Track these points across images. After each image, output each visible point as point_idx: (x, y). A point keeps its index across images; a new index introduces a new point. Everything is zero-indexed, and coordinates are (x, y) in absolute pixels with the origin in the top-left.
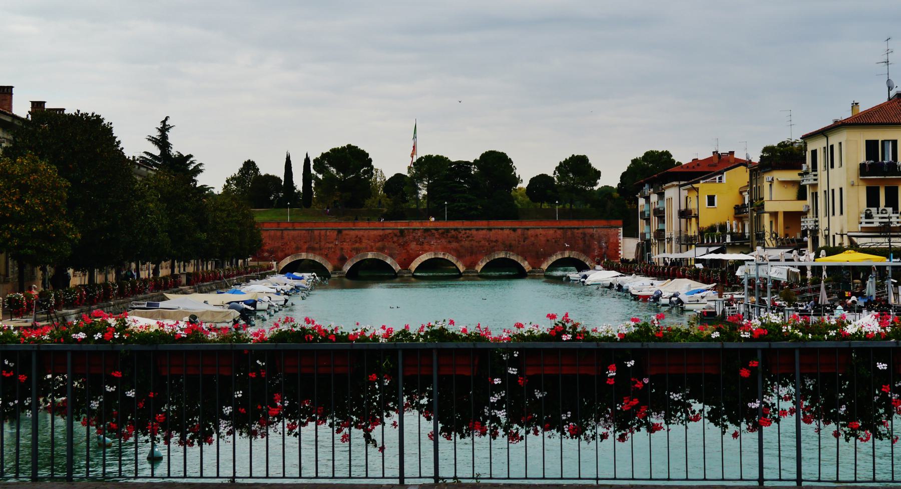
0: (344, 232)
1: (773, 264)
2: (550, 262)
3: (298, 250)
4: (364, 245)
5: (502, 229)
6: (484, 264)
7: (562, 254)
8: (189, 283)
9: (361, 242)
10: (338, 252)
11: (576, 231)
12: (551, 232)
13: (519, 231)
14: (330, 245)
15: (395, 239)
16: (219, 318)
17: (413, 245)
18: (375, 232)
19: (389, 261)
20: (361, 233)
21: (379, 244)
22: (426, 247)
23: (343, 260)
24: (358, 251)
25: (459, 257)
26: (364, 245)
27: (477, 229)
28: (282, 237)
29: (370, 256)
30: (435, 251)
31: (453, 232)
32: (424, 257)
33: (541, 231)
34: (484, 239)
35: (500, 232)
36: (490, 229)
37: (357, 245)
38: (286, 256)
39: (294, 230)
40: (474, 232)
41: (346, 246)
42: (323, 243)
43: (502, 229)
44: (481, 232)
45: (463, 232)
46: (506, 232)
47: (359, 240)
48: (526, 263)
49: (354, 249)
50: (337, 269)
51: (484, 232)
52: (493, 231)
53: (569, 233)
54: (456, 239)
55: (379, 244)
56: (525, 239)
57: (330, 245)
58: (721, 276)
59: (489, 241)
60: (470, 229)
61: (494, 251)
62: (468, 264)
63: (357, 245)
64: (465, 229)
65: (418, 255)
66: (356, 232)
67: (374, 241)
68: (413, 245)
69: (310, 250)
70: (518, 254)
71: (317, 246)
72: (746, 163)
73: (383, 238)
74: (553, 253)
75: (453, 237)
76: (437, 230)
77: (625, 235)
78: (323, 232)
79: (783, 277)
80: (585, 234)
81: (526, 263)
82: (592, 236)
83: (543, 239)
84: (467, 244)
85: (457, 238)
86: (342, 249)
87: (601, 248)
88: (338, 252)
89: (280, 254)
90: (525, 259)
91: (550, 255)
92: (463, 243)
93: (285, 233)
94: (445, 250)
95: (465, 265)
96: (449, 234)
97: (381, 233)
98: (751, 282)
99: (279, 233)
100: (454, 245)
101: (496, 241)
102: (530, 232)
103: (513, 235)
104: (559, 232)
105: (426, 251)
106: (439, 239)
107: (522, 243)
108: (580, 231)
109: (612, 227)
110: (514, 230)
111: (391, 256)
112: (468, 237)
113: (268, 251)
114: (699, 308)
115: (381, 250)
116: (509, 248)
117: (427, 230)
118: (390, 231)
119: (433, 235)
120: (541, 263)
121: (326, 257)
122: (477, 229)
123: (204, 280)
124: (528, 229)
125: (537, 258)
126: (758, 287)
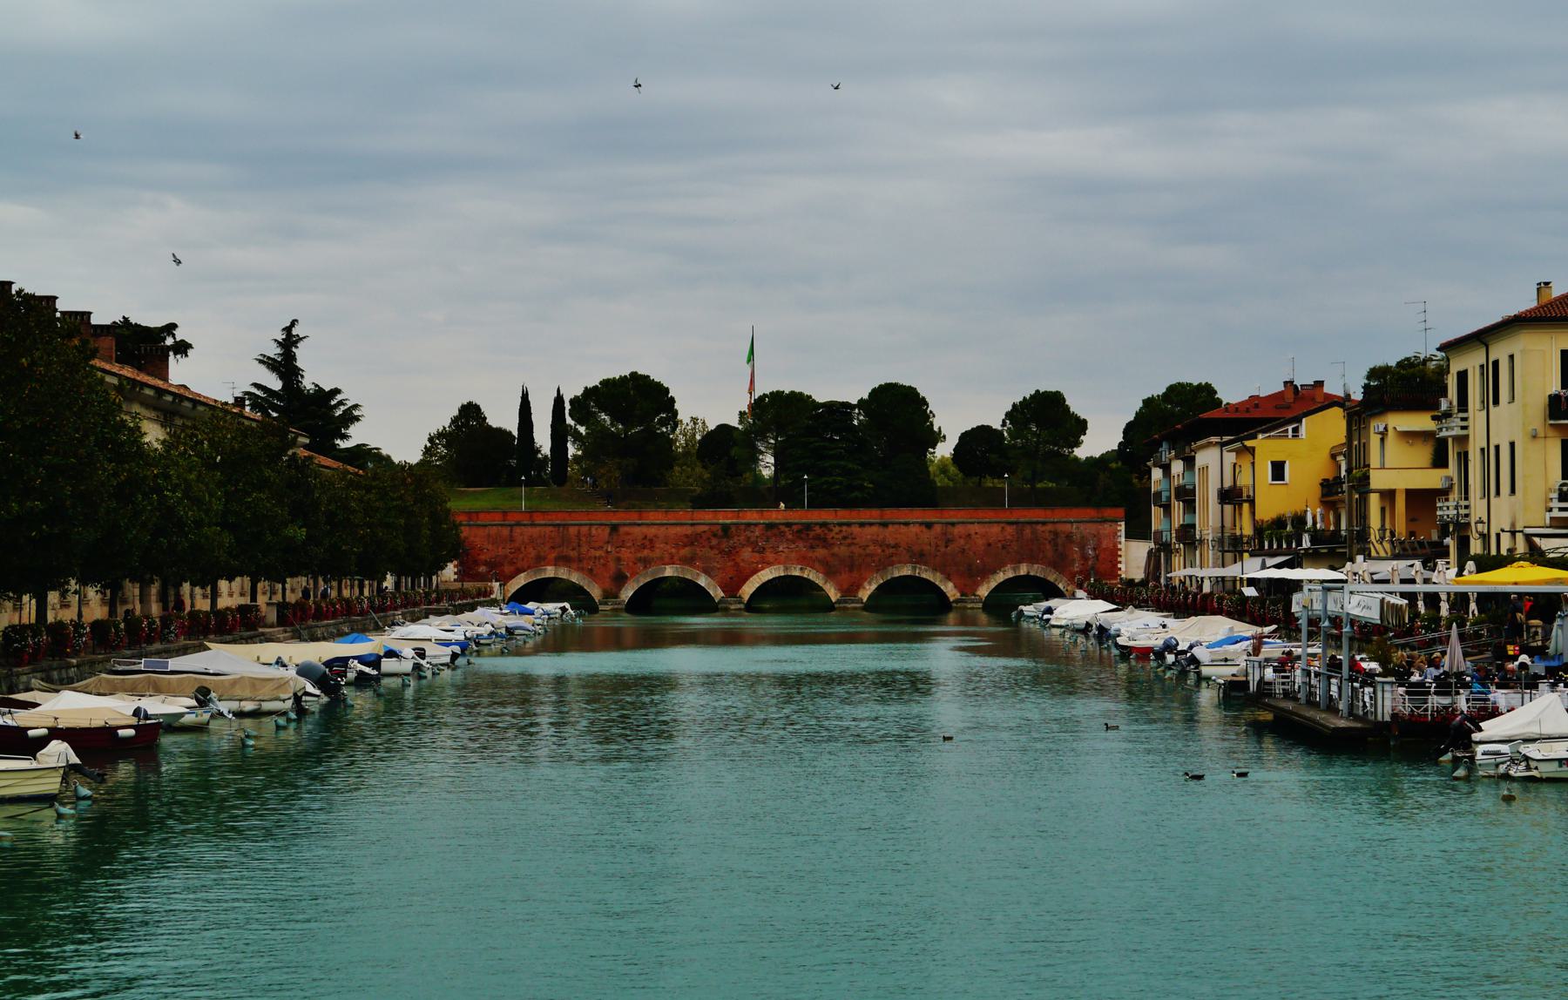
0: (623, 530)
1: (1364, 591)
2: (993, 584)
3: (540, 561)
4: (657, 553)
5: (907, 524)
6: (874, 587)
7: (1014, 569)
8: (282, 621)
9: (652, 548)
10: (612, 565)
11: (1039, 527)
12: (996, 529)
13: (938, 528)
14: (598, 553)
15: (714, 542)
16: (265, 692)
17: (747, 553)
18: (679, 529)
19: (703, 581)
20: (653, 531)
21: (686, 551)
22: (770, 556)
23: (620, 580)
24: (646, 562)
25: (829, 573)
26: (657, 553)
27: (862, 525)
28: (512, 539)
29: (669, 571)
30: (786, 563)
31: (818, 530)
32: (766, 575)
33: (976, 528)
34: (875, 542)
35: (903, 529)
36: (885, 525)
37: (646, 553)
39: (533, 525)
40: (856, 530)
41: (626, 554)
42: (584, 549)
43: (907, 524)
44: (868, 530)
45: (837, 529)
46: (914, 529)
47: (650, 543)
48: (950, 585)
49: (640, 560)
50: (610, 595)
51: (875, 529)
53: (1028, 531)
54: (824, 542)
55: (686, 551)
56: (948, 542)
57: (598, 553)
58: (1270, 607)
59: (883, 544)
60: (849, 525)
61: (892, 564)
63: (646, 553)
64: (840, 525)
65: (755, 571)
66: (644, 529)
67: (677, 546)
68: (747, 553)
69: (562, 560)
70: (935, 569)
71: (573, 554)
72: (1341, 402)
73: (692, 540)
75: (817, 537)
76: (789, 525)
77: (1129, 536)
78: (584, 529)
79: (1374, 615)
80: (1056, 534)
81: (950, 585)
82: (1069, 536)
83: (980, 542)
84: (843, 551)
85: (825, 540)
86: (619, 559)
87: (1085, 558)
88: (612, 565)
89: (507, 569)
90: (949, 578)
91: (994, 572)
92: (836, 549)
93: (518, 530)
94: (804, 561)
95: (840, 589)
96: (812, 534)
97: (689, 530)
98: (1314, 622)
99: (506, 531)
100: (821, 552)
101: (896, 546)
102: (957, 530)
103: (927, 536)
104: (1010, 529)
105: (769, 564)
108: (1049, 527)
109: (1105, 521)
110: (929, 526)
111: (707, 572)
112: (845, 538)
113: (486, 563)
114: (1223, 673)
115: (689, 561)
116: (919, 558)
117: (770, 526)
118: (706, 528)
119: (782, 534)
120: (977, 585)
121: (590, 573)
122: (862, 525)
123: (319, 615)
124: (953, 524)
125: (970, 576)
126: (1330, 629)
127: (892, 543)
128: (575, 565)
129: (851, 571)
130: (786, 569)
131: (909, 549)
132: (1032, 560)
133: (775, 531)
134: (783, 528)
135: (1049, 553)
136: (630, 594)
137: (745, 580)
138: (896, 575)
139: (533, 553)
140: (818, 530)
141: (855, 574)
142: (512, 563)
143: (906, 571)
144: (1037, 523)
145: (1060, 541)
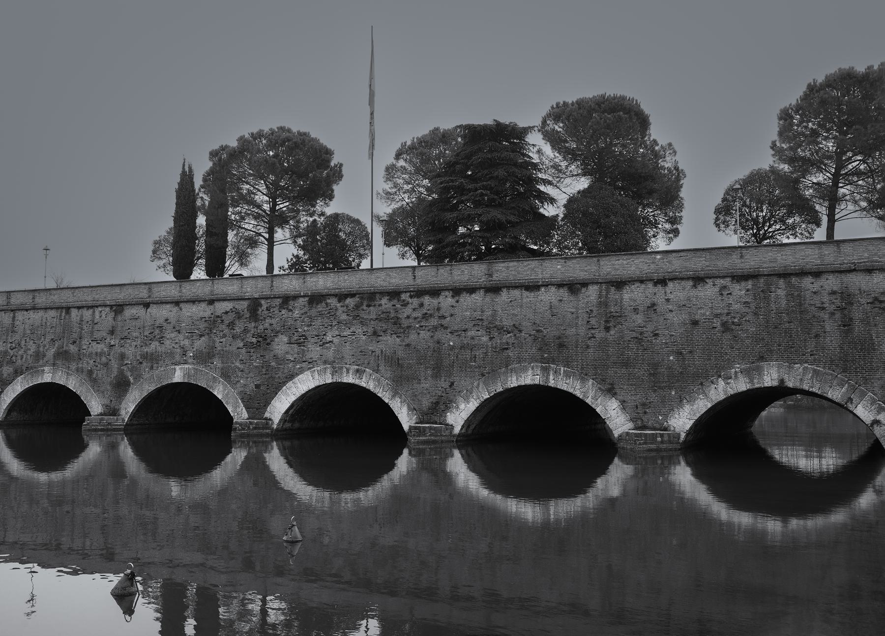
2: (702, 405)
5: (532, 287)
6: (472, 405)
7: (747, 373)
9: (161, 340)
10: (114, 365)
12: (709, 291)
17: (281, 345)
23: (122, 386)
24: (153, 359)
25: (401, 380)
32: (305, 383)
34: (478, 322)
35: (528, 297)
36: (494, 289)
37: (154, 346)
38: (17, 373)
42: (85, 342)
43: (532, 287)
44: (467, 300)
45: (415, 302)
46: (548, 296)
47: (157, 332)
49: (145, 356)
51: (478, 298)
52: (504, 295)
53: (780, 291)
55: (200, 344)
59: (493, 327)
60: (435, 292)
62: (426, 403)
63: (154, 346)
64: (419, 293)
65: (291, 377)
70: (583, 377)
71: (73, 349)
74: (720, 371)
75: (385, 317)
78: (87, 314)
80: (846, 298)
83: (677, 318)
84: (421, 338)
85: (397, 322)
86: (122, 356)
88: (114, 365)
90: (611, 391)
92: (413, 336)
93: (20, 316)
100: (390, 342)
101: (517, 328)
102: (633, 295)
104: (739, 290)
105: (311, 364)
106: (348, 325)
107: (600, 334)
108: (831, 282)
110: (574, 287)
111: (226, 375)
112: (425, 316)
115: (204, 358)
119: (332, 313)
122: (457, 291)
124: (619, 284)
127: (507, 323)
128: (73, 366)
129: (436, 376)
131: (538, 337)
132: (790, 354)
133: (321, 307)
134: (333, 301)
135: (832, 340)
136: (131, 408)
137: (274, 388)
138: (513, 382)
139: (33, 348)
142: (11, 362)
143: (530, 377)
144: (802, 273)
145: (857, 314)
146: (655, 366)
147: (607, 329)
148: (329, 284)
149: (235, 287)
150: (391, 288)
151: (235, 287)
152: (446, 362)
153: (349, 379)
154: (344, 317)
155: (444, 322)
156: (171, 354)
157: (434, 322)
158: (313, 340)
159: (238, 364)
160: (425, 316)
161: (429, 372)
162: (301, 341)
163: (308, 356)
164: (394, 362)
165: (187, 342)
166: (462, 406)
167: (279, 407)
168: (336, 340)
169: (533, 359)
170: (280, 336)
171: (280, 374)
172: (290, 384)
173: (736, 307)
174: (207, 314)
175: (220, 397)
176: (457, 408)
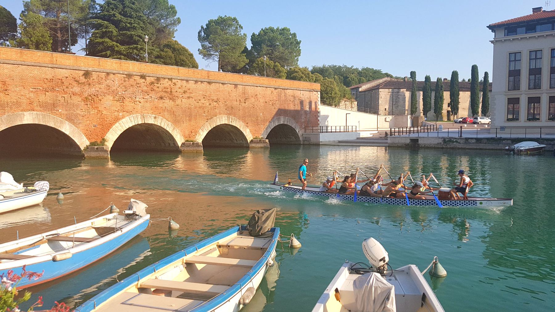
12: (269, 91)
15: (77, 89)
17: (108, 101)
19: (67, 129)
25: (176, 122)
40: (191, 84)
45: (179, 83)
65: (117, 119)
68: (108, 101)
76: (143, 77)
81: (248, 130)
83: (262, 100)
84: (184, 102)
97: (49, 73)
100: (168, 103)
104: (275, 92)
105: (130, 112)
111: (71, 119)
112: (185, 92)
115: (52, 107)
116: (231, 111)
127: (215, 98)
129: (190, 120)
130: (143, 117)
134: (137, 78)
137: (107, 127)
140: (166, 83)
141: (193, 123)
146: (257, 117)
147: (245, 103)
148: (136, 69)
149: (72, 61)
150: (170, 77)
151: (72, 61)
152: (193, 114)
153: (151, 121)
154: (145, 88)
155: (192, 95)
156: (18, 104)
157: (187, 95)
158: (128, 100)
159: (78, 112)
160: (185, 92)
161: (187, 118)
162: (122, 99)
163: (126, 109)
164: (172, 113)
165: (32, 95)
166: (202, 133)
167: (111, 138)
168: (142, 100)
169: (225, 114)
170: (108, 96)
171: (110, 119)
172: (117, 124)
173: (275, 98)
174: (49, 77)
175: (67, 133)
176: (200, 134)
